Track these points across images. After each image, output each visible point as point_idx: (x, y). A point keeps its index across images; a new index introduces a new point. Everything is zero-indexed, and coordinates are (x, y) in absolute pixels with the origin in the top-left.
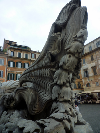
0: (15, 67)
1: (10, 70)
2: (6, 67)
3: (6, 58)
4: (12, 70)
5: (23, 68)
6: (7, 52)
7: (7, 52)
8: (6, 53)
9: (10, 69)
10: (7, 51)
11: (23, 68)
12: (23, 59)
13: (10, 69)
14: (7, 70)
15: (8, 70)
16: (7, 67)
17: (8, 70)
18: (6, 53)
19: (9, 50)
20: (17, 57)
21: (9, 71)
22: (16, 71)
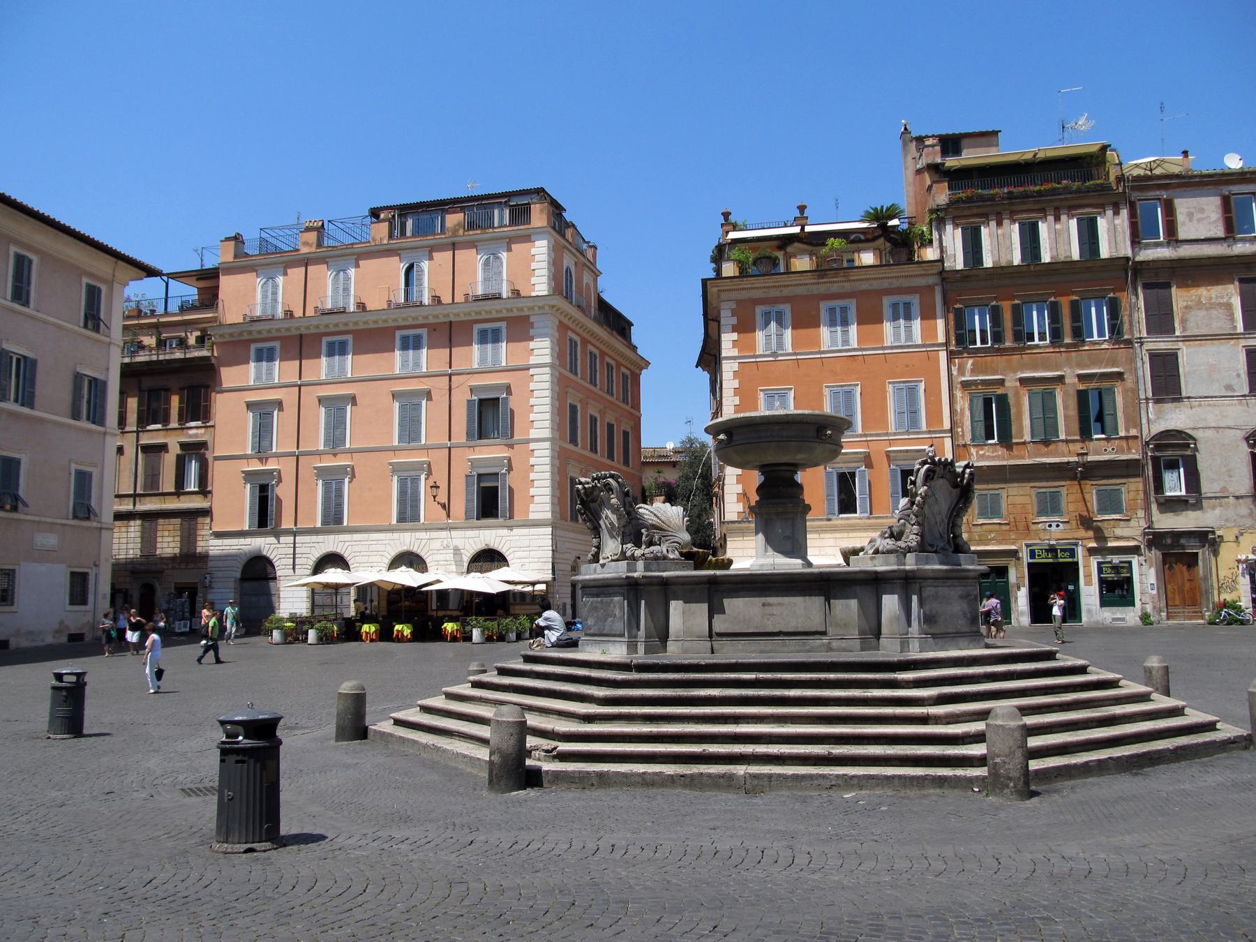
0: (1008, 344)
1: (973, 371)
2: (943, 355)
3: (931, 288)
4: (986, 373)
5: (1068, 340)
6: (936, 243)
7: (936, 243)
8: (930, 254)
9: (970, 361)
10: (935, 235)
11: (1068, 340)
12: (1061, 268)
13: (970, 361)
14: (955, 372)
15: (961, 371)
16: (951, 356)
17: (961, 371)
18: (930, 254)
19: (949, 228)
20: (1011, 266)
21: (967, 378)
22: (1015, 372)
